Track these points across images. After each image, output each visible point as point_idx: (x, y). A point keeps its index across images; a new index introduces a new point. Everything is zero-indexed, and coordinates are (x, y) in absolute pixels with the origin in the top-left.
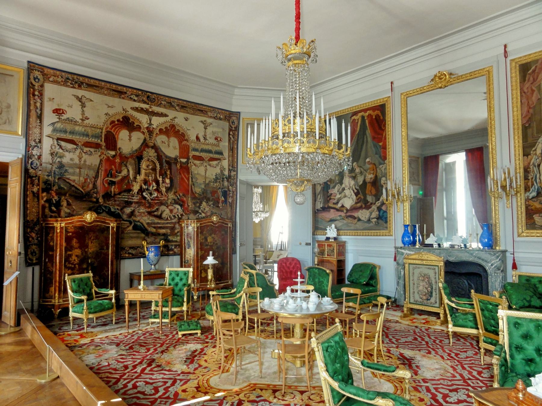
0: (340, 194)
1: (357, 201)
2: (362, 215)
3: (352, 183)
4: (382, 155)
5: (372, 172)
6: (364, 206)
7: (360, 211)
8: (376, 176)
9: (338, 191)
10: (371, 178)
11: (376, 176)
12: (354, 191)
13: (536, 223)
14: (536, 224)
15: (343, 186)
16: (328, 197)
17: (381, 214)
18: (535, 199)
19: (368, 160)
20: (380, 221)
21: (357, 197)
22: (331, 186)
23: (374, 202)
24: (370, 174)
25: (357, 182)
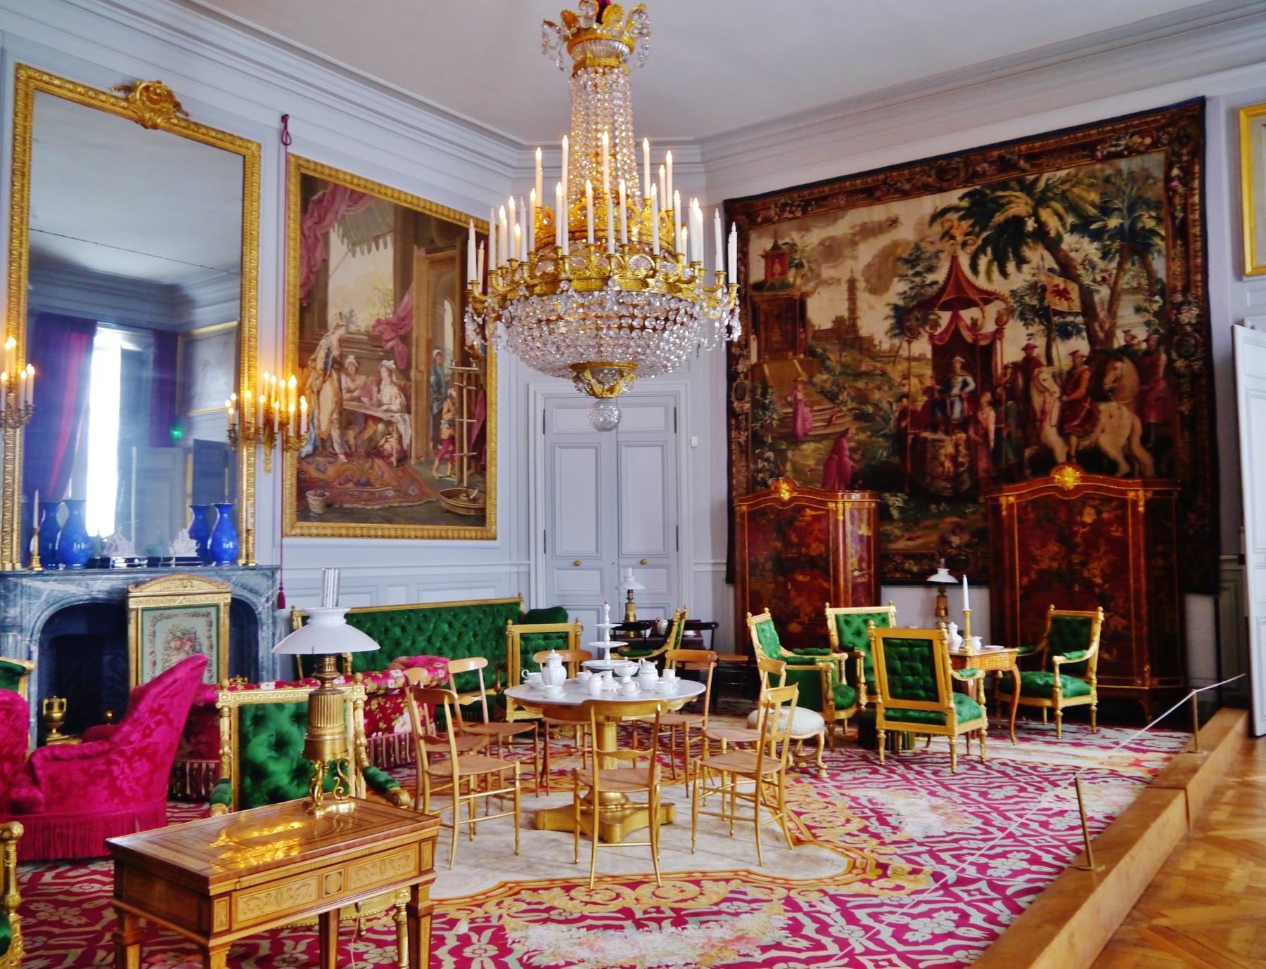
13: (311, 508)
14: (310, 511)
18: (309, 460)
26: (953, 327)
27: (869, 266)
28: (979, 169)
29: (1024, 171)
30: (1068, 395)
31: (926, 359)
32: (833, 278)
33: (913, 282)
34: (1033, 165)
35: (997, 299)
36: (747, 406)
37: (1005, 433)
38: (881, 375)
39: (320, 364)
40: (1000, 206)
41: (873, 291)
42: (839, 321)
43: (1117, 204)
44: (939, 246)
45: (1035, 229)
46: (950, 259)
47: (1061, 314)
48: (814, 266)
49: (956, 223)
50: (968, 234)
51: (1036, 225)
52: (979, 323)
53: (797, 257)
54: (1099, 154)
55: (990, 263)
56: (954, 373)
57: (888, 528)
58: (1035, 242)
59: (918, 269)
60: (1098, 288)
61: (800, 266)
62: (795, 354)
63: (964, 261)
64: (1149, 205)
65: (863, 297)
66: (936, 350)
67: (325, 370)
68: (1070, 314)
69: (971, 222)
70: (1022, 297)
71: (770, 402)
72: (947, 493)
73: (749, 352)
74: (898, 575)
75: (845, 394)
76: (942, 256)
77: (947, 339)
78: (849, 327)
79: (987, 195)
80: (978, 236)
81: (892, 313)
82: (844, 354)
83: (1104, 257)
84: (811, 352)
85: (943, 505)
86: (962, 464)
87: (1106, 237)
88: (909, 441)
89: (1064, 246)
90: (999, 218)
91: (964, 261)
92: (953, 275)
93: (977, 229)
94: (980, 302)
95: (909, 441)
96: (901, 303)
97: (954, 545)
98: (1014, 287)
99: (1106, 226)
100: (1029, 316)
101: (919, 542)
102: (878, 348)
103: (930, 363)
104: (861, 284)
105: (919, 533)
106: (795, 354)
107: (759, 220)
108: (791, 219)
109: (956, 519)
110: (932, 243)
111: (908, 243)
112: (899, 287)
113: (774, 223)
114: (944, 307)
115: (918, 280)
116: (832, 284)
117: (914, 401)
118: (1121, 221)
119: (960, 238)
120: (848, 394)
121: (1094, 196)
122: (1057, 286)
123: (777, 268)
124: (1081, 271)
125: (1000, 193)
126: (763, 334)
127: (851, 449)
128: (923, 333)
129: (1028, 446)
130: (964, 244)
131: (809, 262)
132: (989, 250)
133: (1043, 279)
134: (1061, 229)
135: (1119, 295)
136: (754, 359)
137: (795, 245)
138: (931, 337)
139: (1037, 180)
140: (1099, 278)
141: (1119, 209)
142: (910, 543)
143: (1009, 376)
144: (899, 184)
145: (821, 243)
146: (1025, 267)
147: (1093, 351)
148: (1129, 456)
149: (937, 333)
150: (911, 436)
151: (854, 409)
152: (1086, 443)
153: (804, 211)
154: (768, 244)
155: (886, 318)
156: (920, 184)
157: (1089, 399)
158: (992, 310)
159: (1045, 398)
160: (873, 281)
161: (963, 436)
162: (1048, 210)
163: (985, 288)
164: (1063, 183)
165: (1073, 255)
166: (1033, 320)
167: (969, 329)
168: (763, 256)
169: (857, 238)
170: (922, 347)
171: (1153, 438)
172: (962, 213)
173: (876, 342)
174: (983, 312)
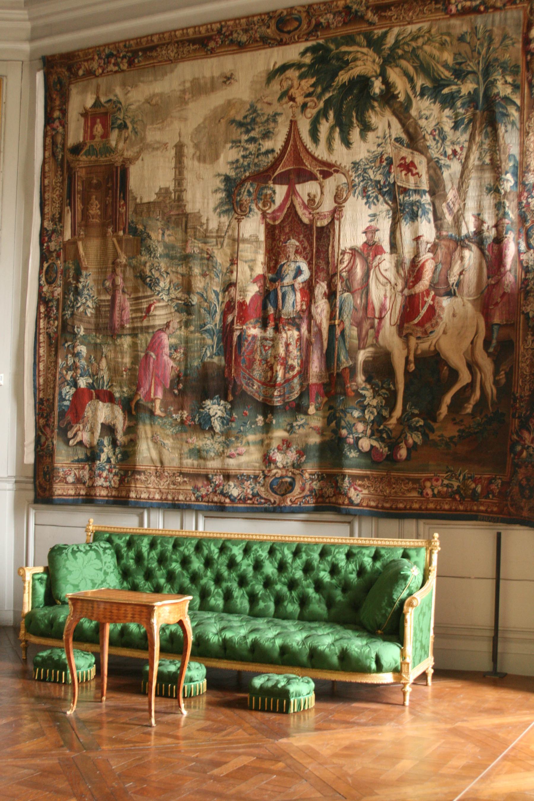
26: (289, 203)
27: (198, 130)
28: (322, 20)
29: (371, 24)
30: (409, 289)
31: (257, 241)
32: (159, 142)
33: (245, 149)
34: (381, 18)
35: (337, 171)
36: (58, 291)
37: (338, 332)
38: (208, 259)
40: (345, 64)
41: (202, 159)
42: (164, 192)
43: (471, 66)
44: (276, 107)
45: (382, 91)
46: (288, 123)
47: (405, 191)
48: (139, 128)
49: (296, 83)
50: (309, 95)
51: (383, 87)
52: (317, 200)
53: (121, 116)
54: (453, 8)
55: (332, 129)
56: (288, 258)
57: (208, 442)
58: (382, 107)
59: (252, 134)
60: (448, 162)
61: (123, 127)
62: (115, 231)
63: (304, 127)
64: (505, 69)
68: (417, 191)
69: (313, 81)
70: (365, 171)
71: (84, 287)
73: (62, 227)
75: (168, 280)
76: (280, 119)
78: (174, 201)
79: (331, 51)
80: (319, 97)
81: (222, 186)
82: (167, 233)
83: (455, 127)
84: (134, 231)
86: (292, 368)
87: (459, 104)
88: (235, 339)
89: (413, 112)
90: (343, 77)
91: (304, 127)
92: (291, 142)
93: (319, 90)
94: (319, 176)
95: (235, 339)
96: (232, 174)
97: (279, 465)
98: (357, 159)
99: (459, 91)
100: (371, 191)
102: (205, 227)
103: (263, 246)
104: (189, 151)
106: (115, 231)
107: (81, 73)
108: (116, 72)
110: (270, 104)
111: (242, 103)
113: (97, 77)
115: (252, 147)
116: (157, 149)
117: (244, 291)
118: (476, 86)
119: (300, 100)
120: (170, 282)
121: (448, 57)
122: (403, 158)
123: (99, 129)
124: (430, 142)
125: (344, 49)
126: (79, 206)
127: (171, 347)
128: (256, 210)
129: (364, 348)
130: (304, 106)
131: (133, 122)
132: (331, 114)
133: (389, 150)
134: (410, 93)
135: (470, 172)
136: (68, 235)
137: (120, 103)
138: (264, 215)
139: (385, 35)
140: (449, 152)
141: (474, 73)
143: (346, 264)
144: (235, 35)
145: (148, 101)
146: (371, 135)
147: (439, 237)
148: (472, 366)
149: (269, 211)
150: (237, 333)
151: (177, 299)
152: (425, 346)
153: (131, 63)
154: (90, 102)
155: (216, 191)
156: (258, 35)
157: (433, 293)
158: (331, 184)
159: (386, 290)
160: (203, 147)
161: (296, 333)
162: (397, 70)
163: (325, 159)
164: (415, 38)
165: (423, 123)
166: (376, 198)
167: (306, 207)
168: (82, 115)
169: (187, 96)
171: (494, 342)
172: (303, 70)
173: (204, 220)
174: (322, 187)
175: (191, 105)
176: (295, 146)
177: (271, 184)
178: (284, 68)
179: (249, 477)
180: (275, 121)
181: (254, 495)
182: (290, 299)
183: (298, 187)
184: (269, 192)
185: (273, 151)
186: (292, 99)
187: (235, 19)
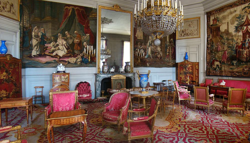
0: (54, 48)
1: (67, 53)
2: (71, 60)
3: (64, 42)
4: (84, 31)
5: (78, 38)
6: (72, 56)
7: (70, 58)
8: (81, 41)
9: (53, 46)
10: (77, 42)
11: (81, 41)
12: (65, 47)
15: (58, 43)
16: (44, 48)
17: (83, 60)
19: (75, 32)
20: (83, 64)
21: (68, 51)
22: (48, 42)
23: (79, 54)
24: (77, 39)
25: (68, 42)
27: (231, 20)
31: (241, 36)
33: (239, 22)
39: (148, 45)
44: (244, 14)
65: (230, 25)
66: (243, 34)
67: (149, 45)
72: (245, 61)
74: (235, 75)
76: (245, 16)
77: (245, 32)
81: (235, 28)
85: (244, 63)
86: (248, 55)
96: (237, 26)
101: (239, 69)
104: (229, 23)
105: (239, 68)
109: (246, 66)
110: (243, 14)
111: (238, 14)
112: (236, 23)
114: (245, 26)
115: (240, 21)
117: (239, 44)
138: (242, 32)
142: (237, 70)
160: (232, 22)
161: (248, 50)
170: (241, 34)
173: (232, 33)
175: (229, 16)
176: (248, 20)
177: (243, 26)
178: (245, 7)
179: (240, 72)
180: (244, 16)
181: (241, 75)
182: (247, 44)
183: (248, 26)
184: (243, 28)
185: (244, 21)
186: (247, 12)
187: (236, 1)
